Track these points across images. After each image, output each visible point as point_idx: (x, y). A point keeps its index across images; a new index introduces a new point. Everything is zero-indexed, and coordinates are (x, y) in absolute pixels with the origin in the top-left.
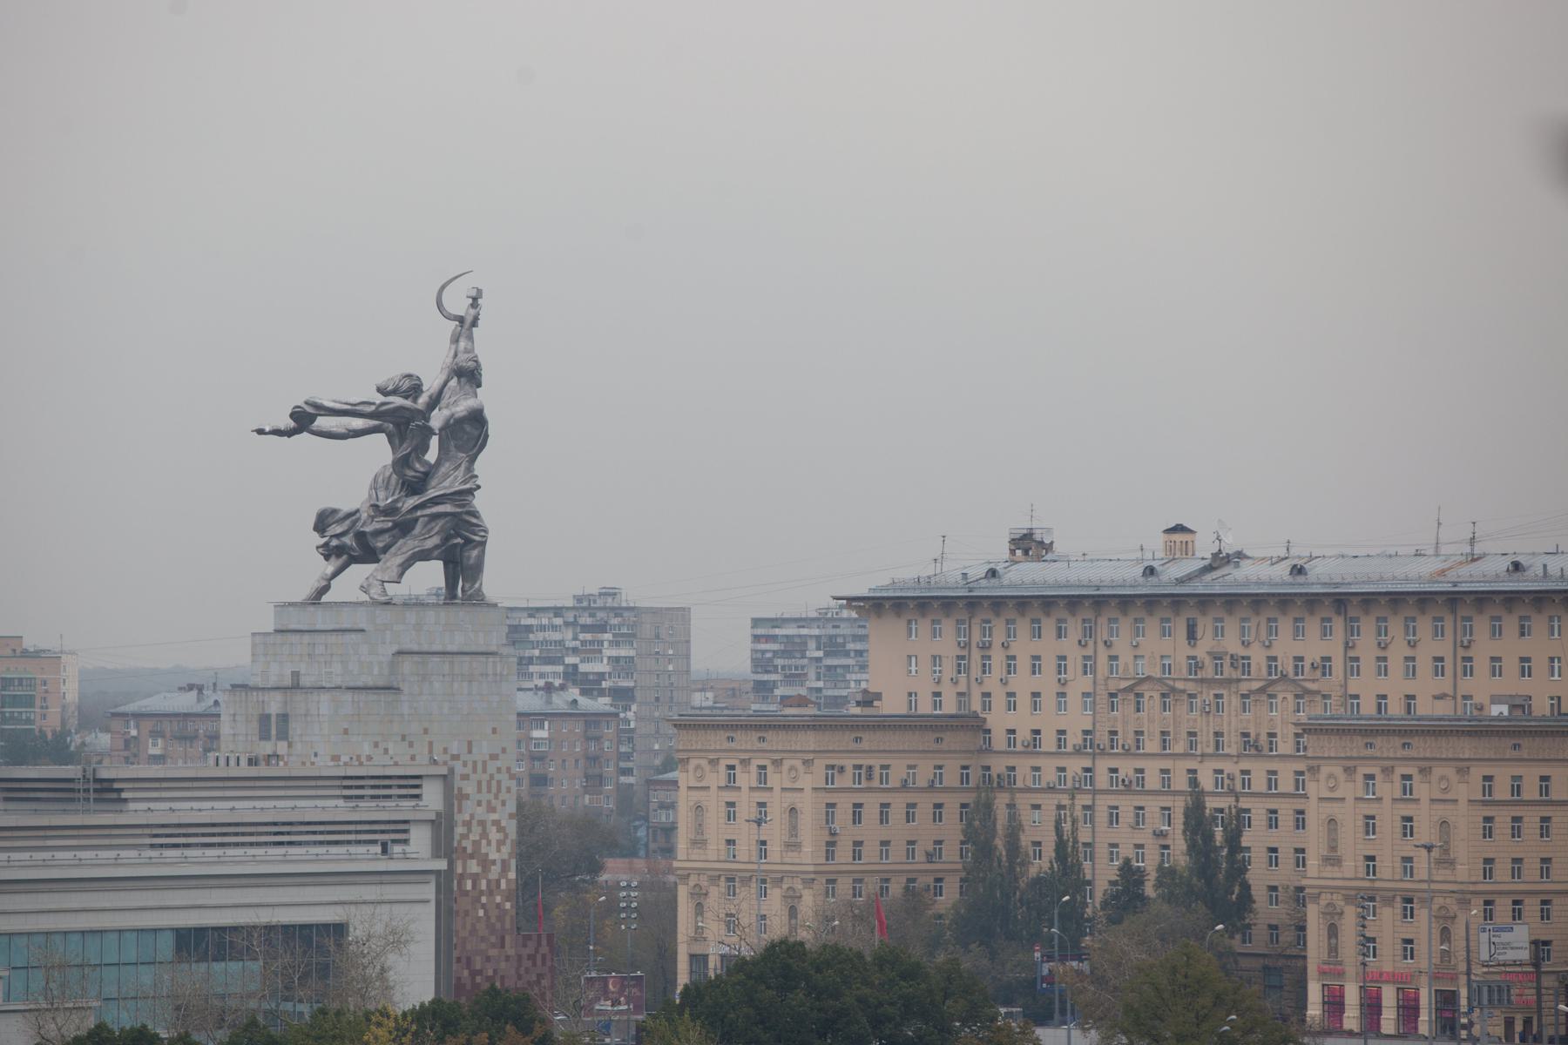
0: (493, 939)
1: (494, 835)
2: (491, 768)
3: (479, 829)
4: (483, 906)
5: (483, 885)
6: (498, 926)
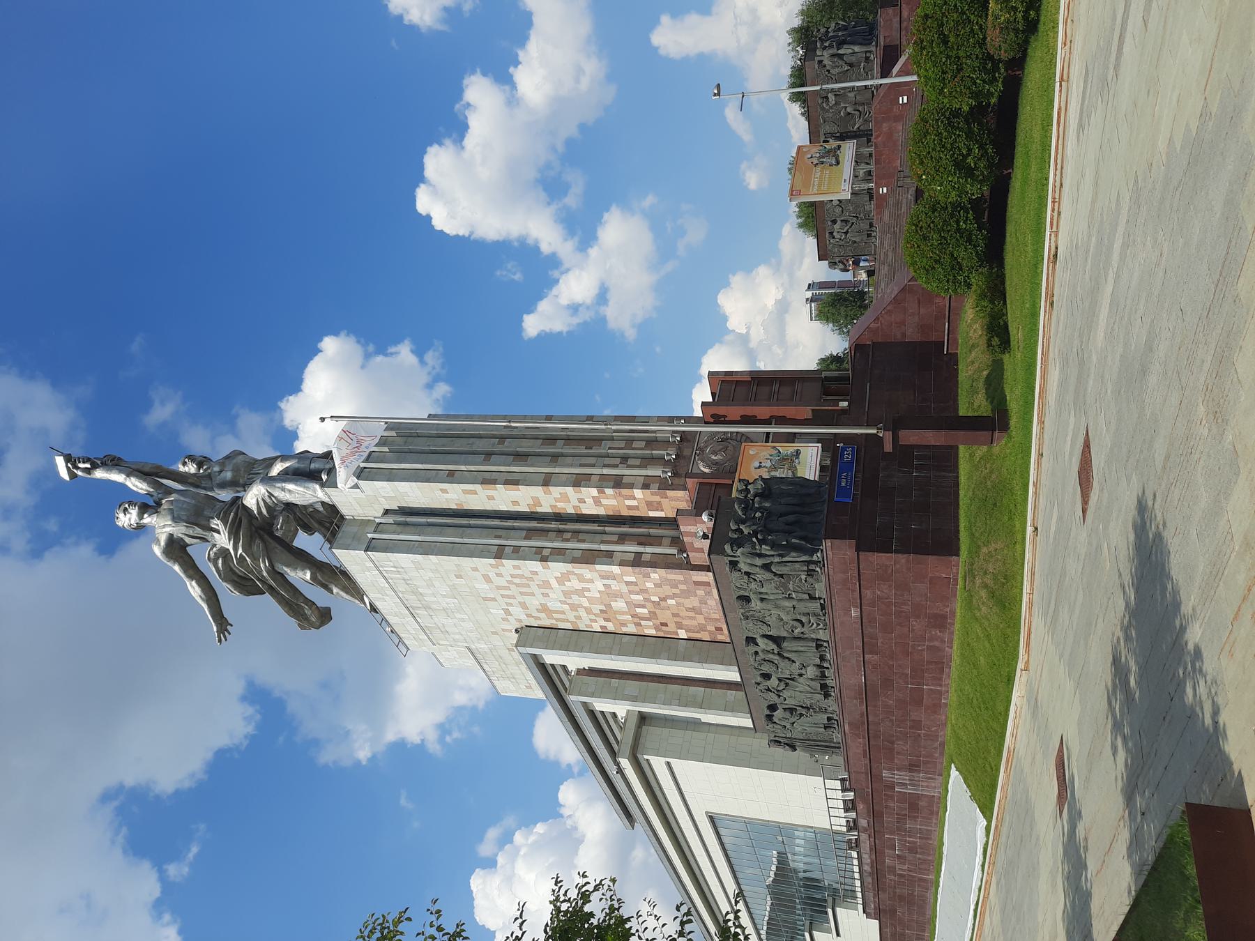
0: (701, 593)
2: (502, 582)
5: (638, 598)
6: (683, 587)
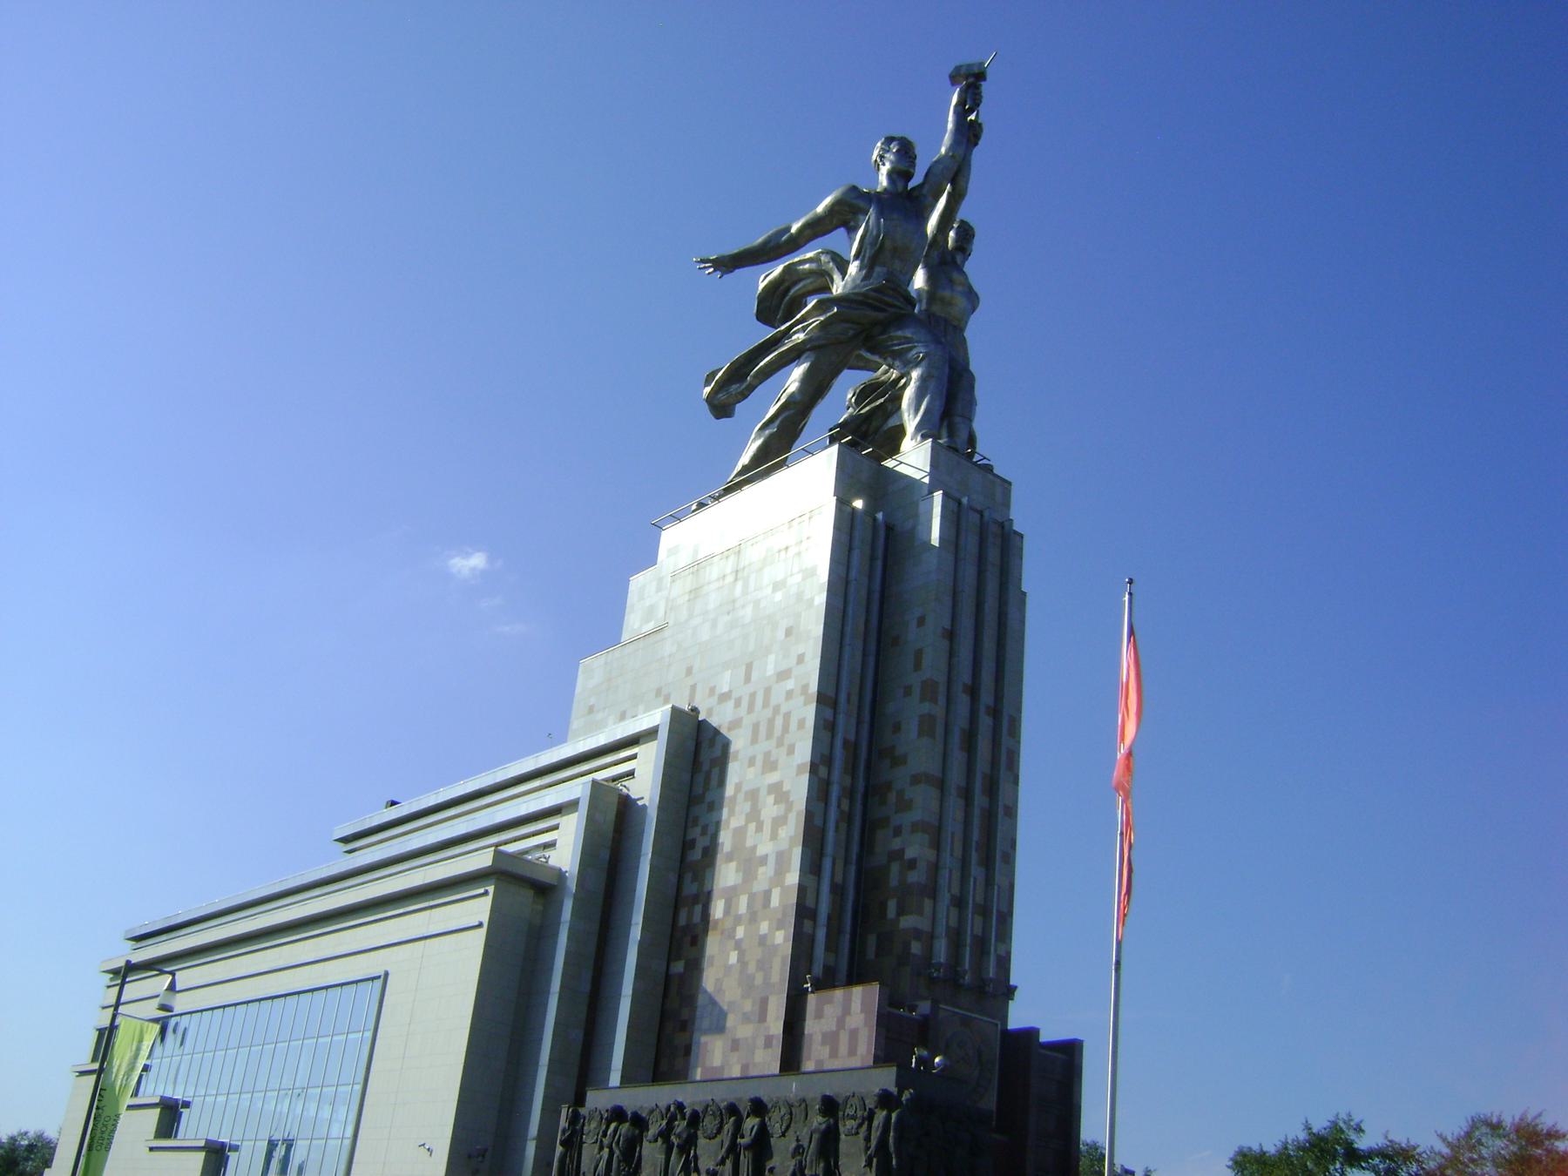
0: (748, 1006)
1: (770, 809)
2: (777, 697)
3: (747, 807)
4: (738, 945)
6: (759, 980)
